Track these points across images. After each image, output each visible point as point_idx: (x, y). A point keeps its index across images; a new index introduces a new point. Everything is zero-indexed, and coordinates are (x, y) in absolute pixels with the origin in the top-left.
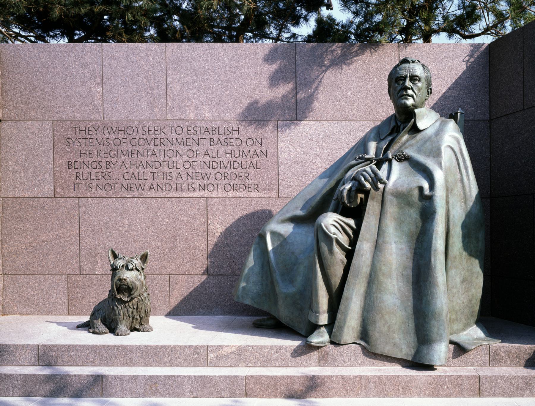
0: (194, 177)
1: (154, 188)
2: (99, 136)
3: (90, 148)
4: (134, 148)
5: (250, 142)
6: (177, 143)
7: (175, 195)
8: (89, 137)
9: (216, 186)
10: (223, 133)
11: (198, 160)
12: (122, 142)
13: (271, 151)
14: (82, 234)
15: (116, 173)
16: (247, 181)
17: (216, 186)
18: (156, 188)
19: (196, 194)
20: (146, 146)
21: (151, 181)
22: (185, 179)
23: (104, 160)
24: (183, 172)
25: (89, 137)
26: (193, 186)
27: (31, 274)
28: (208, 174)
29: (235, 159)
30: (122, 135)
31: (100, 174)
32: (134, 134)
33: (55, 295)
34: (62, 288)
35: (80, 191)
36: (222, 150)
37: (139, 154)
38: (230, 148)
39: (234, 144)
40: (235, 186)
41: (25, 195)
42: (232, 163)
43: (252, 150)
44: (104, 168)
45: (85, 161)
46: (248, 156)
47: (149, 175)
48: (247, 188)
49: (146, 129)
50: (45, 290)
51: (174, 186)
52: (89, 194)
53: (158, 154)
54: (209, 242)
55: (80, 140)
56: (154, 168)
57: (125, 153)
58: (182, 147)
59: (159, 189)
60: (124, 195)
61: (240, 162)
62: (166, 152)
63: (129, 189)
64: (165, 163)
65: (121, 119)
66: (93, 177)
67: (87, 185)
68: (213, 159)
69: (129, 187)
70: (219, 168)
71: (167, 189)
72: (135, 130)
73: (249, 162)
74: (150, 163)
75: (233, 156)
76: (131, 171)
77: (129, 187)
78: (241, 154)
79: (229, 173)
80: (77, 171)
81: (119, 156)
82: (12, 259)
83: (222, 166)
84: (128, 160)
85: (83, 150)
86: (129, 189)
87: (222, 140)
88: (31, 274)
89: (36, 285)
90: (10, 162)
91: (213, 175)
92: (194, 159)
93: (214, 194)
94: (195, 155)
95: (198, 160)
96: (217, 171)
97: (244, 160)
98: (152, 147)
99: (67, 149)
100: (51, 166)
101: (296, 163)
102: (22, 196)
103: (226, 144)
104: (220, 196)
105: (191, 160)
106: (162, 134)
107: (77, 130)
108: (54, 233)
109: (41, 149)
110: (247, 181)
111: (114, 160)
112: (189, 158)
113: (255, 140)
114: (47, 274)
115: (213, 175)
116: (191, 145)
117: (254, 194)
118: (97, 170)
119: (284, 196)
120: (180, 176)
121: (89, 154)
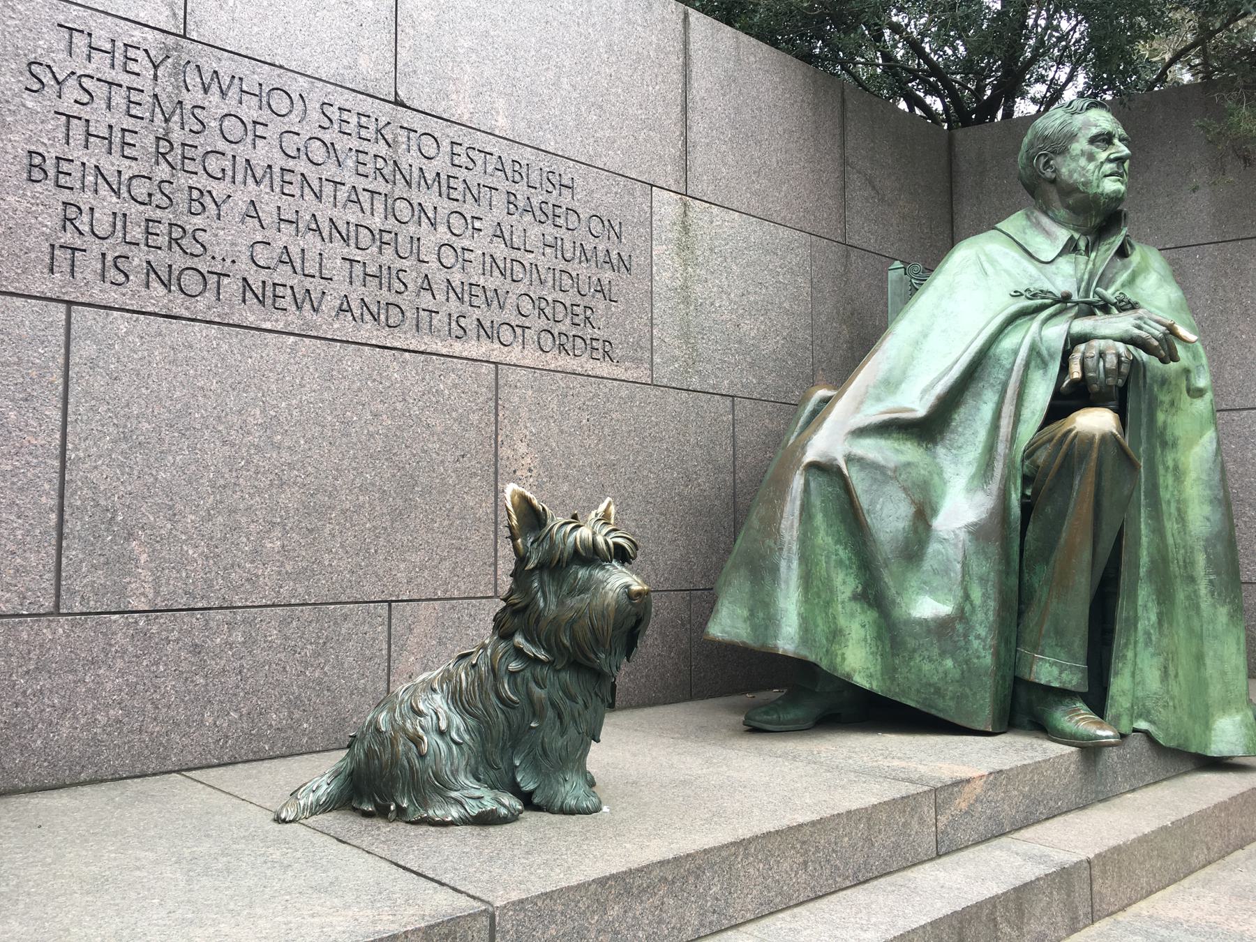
0: (466, 298)
3: (128, 123)
4: (291, 164)
5: (596, 226)
8: (125, 79)
9: (519, 331)
13: (639, 260)
14: (76, 449)
18: (357, 312)
19: (473, 348)
21: (344, 288)
22: (441, 297)
23: (183, 180)
24: (438, 277)
25: (125, 79)
26: (463, 322)
30: (250, 111)
31: (163, 228)
32: (294, 117)
35: (78, 276)
36: (535, 231)
44: (183, 207)
47: (335, 267)
49: (334, 113)
52: (113, 296)
53: (367, 206)
55: (87, 83)
56: (352, 242)
57: (259, 174)
59: (367, 317)
60: (251, 319)
61: (574, 274)
62: (390, 201)
63: (269, 301)
64: (386, 237)
66: (136, 233)
67: (109, 258)
69: (269, 293)
71: (391, 322)
73: (594, 279)
75: (559, 256)
76: (280, 241)
77: (269, 293)
79: (550, 299)
80: (66, 196)
85: (100, 119)
86: (267, 297)
87: (535, 202)
91: (512, 299)
92: (466, 243)
93: (514, 354)
95: (479, 245)
103: (543, 218)
107: (80, 41)
111: (219, 190)
112: (454, 238)
113: (606, 223)
117: (604, 368)
118: (150, 212)
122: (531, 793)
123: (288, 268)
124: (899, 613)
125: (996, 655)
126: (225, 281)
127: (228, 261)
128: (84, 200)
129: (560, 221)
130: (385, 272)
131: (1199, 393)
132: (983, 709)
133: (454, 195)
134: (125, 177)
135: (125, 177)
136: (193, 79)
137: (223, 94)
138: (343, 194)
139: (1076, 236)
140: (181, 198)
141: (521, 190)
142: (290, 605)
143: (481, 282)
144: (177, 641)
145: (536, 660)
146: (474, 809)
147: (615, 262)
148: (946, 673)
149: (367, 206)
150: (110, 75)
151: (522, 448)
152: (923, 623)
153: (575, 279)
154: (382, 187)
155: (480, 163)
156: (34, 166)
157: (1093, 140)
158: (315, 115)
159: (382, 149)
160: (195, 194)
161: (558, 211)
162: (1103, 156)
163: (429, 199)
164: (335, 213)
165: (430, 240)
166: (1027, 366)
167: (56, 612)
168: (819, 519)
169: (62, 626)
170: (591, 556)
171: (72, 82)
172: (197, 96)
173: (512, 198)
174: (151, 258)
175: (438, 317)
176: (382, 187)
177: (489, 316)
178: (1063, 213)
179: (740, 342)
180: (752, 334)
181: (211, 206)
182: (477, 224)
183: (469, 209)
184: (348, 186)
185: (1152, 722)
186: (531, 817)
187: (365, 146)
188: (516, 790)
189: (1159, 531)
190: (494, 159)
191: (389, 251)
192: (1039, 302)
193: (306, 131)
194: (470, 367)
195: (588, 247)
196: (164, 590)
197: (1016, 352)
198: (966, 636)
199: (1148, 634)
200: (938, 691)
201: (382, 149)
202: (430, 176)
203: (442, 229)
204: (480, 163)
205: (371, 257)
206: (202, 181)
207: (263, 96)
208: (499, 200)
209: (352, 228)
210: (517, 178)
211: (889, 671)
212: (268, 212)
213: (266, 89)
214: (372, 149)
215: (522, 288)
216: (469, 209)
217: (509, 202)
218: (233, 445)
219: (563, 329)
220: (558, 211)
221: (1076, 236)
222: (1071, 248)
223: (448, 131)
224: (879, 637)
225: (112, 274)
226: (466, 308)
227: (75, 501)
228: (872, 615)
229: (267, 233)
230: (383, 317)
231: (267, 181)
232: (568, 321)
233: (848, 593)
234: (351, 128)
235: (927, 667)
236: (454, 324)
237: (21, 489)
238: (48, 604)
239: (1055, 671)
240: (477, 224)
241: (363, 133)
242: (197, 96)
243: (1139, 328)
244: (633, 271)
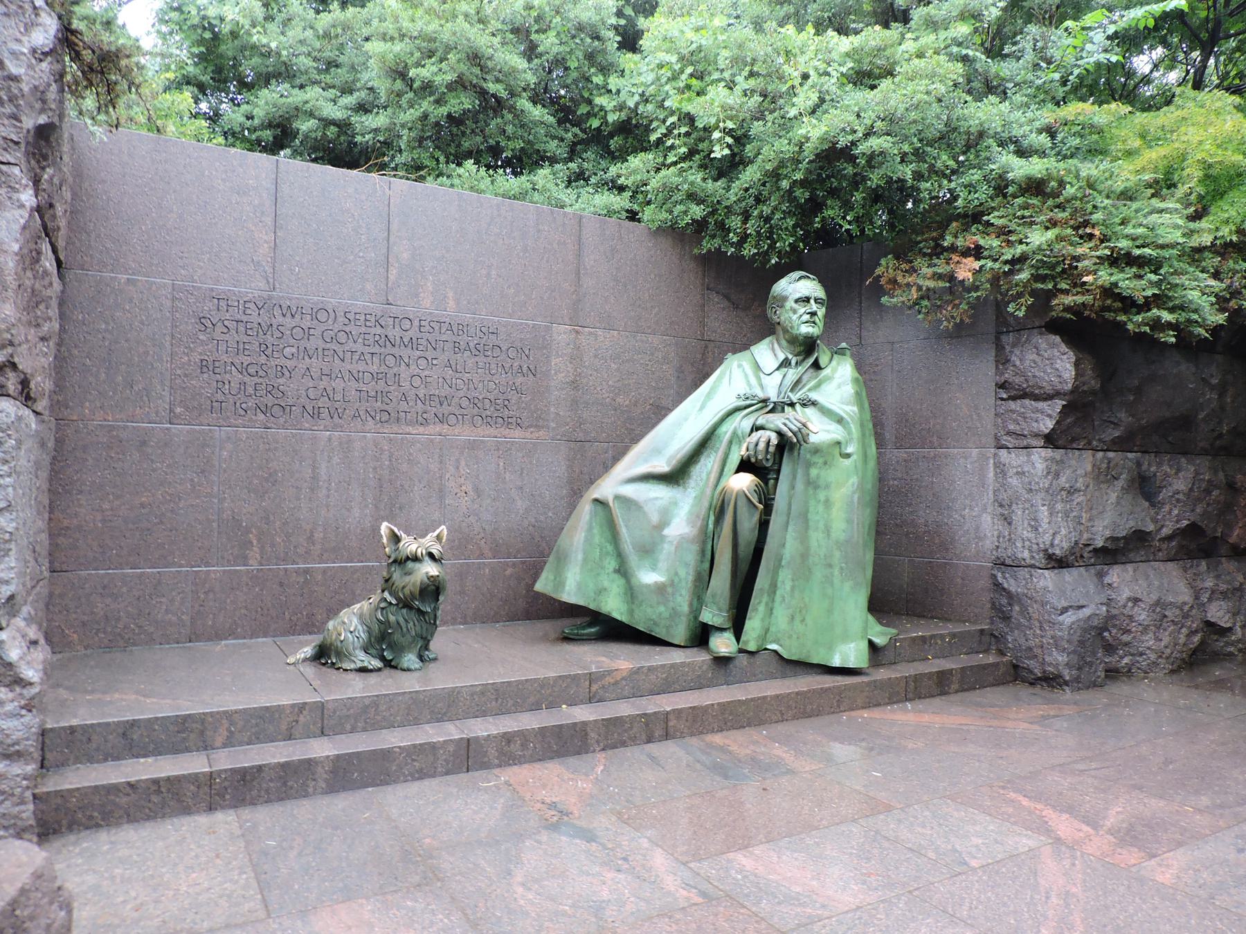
2: (265, 319)
4: (328, 346)
5: (512, 353)
9: (460, 417)
17: (460, 417)
18: (364, 418)
25: (245, 318)
30: (307, 323)
32: (330, 321)
45: (237, 362)
49: (351, 316)
53: (369, 362)
55: (226, 323)
58: (409, 351)
59: (369, 419)
63: (316, 416)
66: (250, 390)
67: (238, 404)
74: (355, 372)
76: (322, 385)
82: (71, 540)
87: (471, 344)
92: (426, 373)
103: (477, 353)
106: (378, 326)
122: (391, 660)
123: (326, 398)
124: (633, 581)
125: (691, 605)
126: (294, 408)
130: (379, 394)
131: (848, 456)
132: (680, 633)
134: (245, 365)
135: (245, 365)
136: (277, 312)
138: (356, 357)
139: (790, 357)
140: (272, 372)
141: (463, 340)
145: (390, 603)
146: (359, 665)
148: (660, 614)
150: (238, 317)
152: (648, 586)
154: (376, 349)
155: (437, 328)
157: (796, 301)
158: (341, 319)
159: (378, 330)
160: (279, 368)
161: (486, 348)
162: (803, 310)
163: (405, 352)
165: (405, 373)
166: (730, 443)
168: (595, 531)
170: (416, 559)
172: (280, 319)
173: (457, 345)
176: (376, 349)
178: (784, 343)
181: (287, 373)
182: (435, 362)
183: (429, 354)
184: (359, 353)
185: (781, 646)
186: (387, 671)
187: (369, 330)
188: (383, 659)
189: (804, 539)
190: (447, 324)
191: (382, 383)
192: (748, 402)
193: (337, 327)
195: (507, 366)
197: (726, 432)
198: (673, 594)
199: (783, 598)
200: (655, 624)
201: (378, 330)
202: (406, 340)
204: (437, 328)
205: (371, 387)
206: (283, 362)
208: (449, 346)
209: (361, 374)
210: (461, 333)
211: (631, 612)
212: (315, 372)
213: (315, 310)
214: (373, 331)
215: (461, 393)
216: (429, 354)
219: (489, 413)
220: (486, 348)
221: (790, 357)
222: (785, 363)
224: (625, 594)
228: (622, 581)
230: (378, 418)
231: (315, 356)
232: (492, 409)
233: (611, 569)
234: (362, 322)
235: (649, 610)
236: (420, 418)
239: (711, 615)
240: (435, 362)
242: (280, 319)
243: (785, 425)
244: (538, 376)
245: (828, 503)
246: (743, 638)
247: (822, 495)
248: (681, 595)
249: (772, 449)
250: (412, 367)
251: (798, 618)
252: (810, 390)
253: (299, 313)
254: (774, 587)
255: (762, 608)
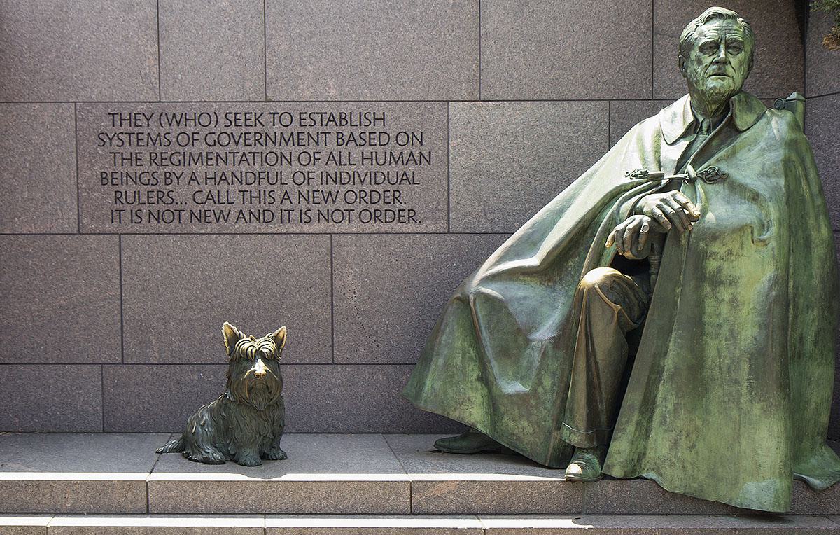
0: (311, 199)
1: (244, 217)
2: (154, 129)
3: (138, 149)
4: (211, 149)
5: (403, 139)
6: (283, 141)
7: (280, 230)
8: (136, 130)
9: (346, 213)
10: (358, 124)
11: (318, 169)
12: (192, 139)
13: (437, 154)
14: (126, 295)
15: (181, 192)
16: (397, 205)
17: (346, 213)
18: (247, 218)
19: (315, 227)
20: (232, 147)
21: (241, 206)
22: (295, 201)
23: (162, 170)
24: (293, 191)
25: (136, 130)
26: (309, 213)
27: (42, 364)
28: (334, 193)
29: (378, 168)
30: (190, 128)
31: (155, 194)
32: (212, 125)
33: (82, 399)
34: (93, 386)
35: (122, 222)
36: (356, 153)
37: (220, 160)
38: (371, 149)
39: (376, 142)
40: (378, 213)
41: (30, 229)
42: (373, 175)
43: (406, 152)
44: (162, 183)
45: (131, 172)
46: (400, 163)
47: (236, 197)
48: (398, 216)
49: (231, 117)
50: (65, 390)
51: (277, 215)
52: (136, 228)
53: (251, 161)
54: (335, 308)
55: (122, 136)
56: (244, 182)
57: (196, 158)
58: (290, 147)
59: (253, 219)
60: (195, 229)
61: (386, 172)
62: (264, 155)
63: (203, 220)
64: (262, 175)
65: (189, 100)
66: (144, 199)
67: (134, 212)
68: (342, 168)
69: (203, 215)
70: (351, 183)
71: (266, 220)
72: (214, 119)
73: (401, 173)
74: (238, 175)
75: (374, 162)
76: (207, 189)
77: (203, 215)
78: (388, 159)
79: (368, 191)
80: (116, 189)
81: (187, 163)
82: (10, 337)
83: (357, 179)
84: (201, 170)
85: (127, 151)
86: (202, 218)
87: (356, 135)
88: (42, 364)
89: (51, 381)
90: (6, 174)
91: (341, 195)
92: (310, 168)
93: (344, 227)
94: (312, 162)
95: (318, 169)
96: (348, 187)
97: (392, 169)
98: (242, 148)
99: (100, 152)
100: (74, 180)
101: (479, 173)
102: (25, 232)
103: (363, 142)
104: (354, 230)
105: (305, 170)
106: (258, 124)
107: (117, 118)
108: (79, 295)
109: (56, 151)
110: (397, 205)
111: (178, 170)
112: (303, 167)
113: (410, 135)
114: (69, 364)
115: (341, 195)
116: (306, 144)
117: (409, 227)
118: (149, 188)
119: (459, 230)
120: (287, 196)
121: (135, 159)
126: (183, 213)
127: (184, 203)
128: (123, 188)
129: (376, 142)
133: (302, 142)
137: (178, 124)
138: (238, 158)
142: (219, 364)
143: (321, 188)
144: (170, 377)
147: (418, 159)
149: (251, 161)
151: (350, 281)
153: (387, 177)
156: (104, 179)
158: (222, 121)
164: (235, 169)
167: (122, 363)
169: (125, 369)
171: (116, 138)
174: (151, 209)
175: (294, 212)
177: (324, 208)
179: (531, 194)
180: (543, 187)
187: (250, 130)
194: (314, 238)
196: (163, 355)
203: (295, 163)
204: (318, 121)
207: (197, 119)
208: (332, 139)
209: (244, 175)
214: (253, 130)
215: (348, 187)
217: (338, 139)
218: (189, 290)
223: (297, 107)
225: (136, 219)
226: (310, 205)
227: (126, 317)
229: (201, 186)
237: (107, 314)
238: (119, 360)
241: (248, 123)
245: (734, 302)
246: (608, 462)
247: (726, 294)
248: (546, 409)
249: (642, 239)
250: (295, 163)
251: (684, 443)
252: (718, 161)
253: (183, 119)
254: (648, 405)
255: (631, 428)
